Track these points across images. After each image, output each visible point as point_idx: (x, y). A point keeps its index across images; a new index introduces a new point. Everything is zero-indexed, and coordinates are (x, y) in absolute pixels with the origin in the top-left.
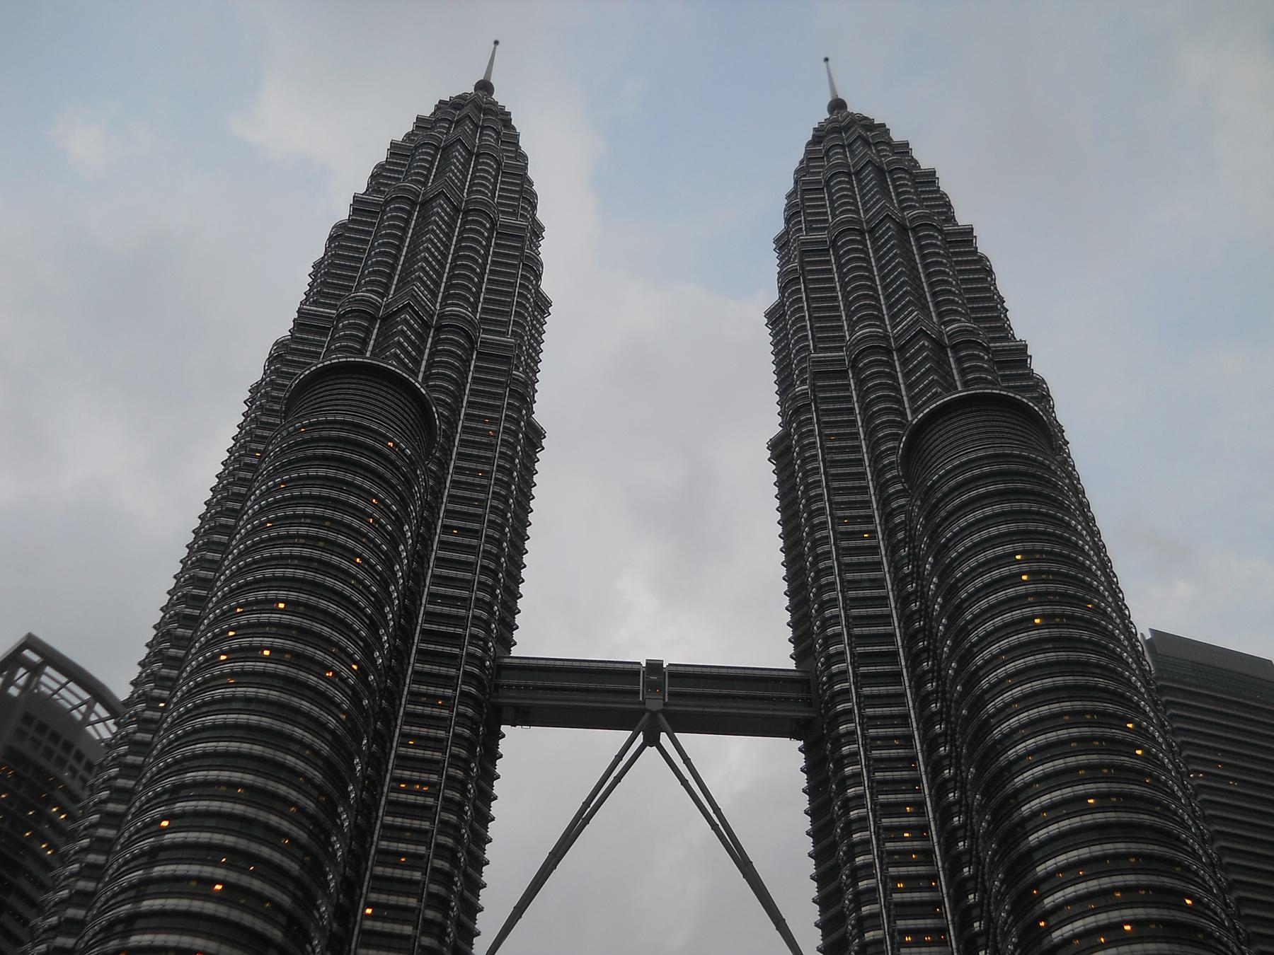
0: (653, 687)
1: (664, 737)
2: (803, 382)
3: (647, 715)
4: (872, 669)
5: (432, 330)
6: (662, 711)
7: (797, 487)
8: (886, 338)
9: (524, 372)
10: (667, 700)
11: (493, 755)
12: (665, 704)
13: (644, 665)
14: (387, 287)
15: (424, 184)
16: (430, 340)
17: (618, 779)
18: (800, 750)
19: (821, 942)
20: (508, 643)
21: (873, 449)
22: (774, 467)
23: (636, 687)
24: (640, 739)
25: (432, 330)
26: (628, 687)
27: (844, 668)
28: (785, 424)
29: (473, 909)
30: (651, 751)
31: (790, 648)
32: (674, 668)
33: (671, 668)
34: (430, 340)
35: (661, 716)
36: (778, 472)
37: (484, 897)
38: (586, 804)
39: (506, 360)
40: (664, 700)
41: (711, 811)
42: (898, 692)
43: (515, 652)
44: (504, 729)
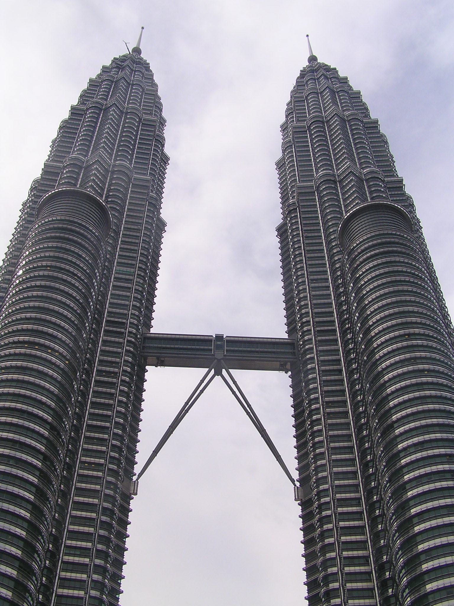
0: (218, 347)
1: (224, 372)
2: (293, 198)
3: (216, 361)
4: (324, 338)
5: (110, 173)
6: (223, 359)
7: (291, 263)
8: (334, 176)
9: (156, 193)
10: (225, 354)
13: (214, 337)
14: (87, 152)
15: (106, 100)
17: (202, 391)
18: (289, 377)
19: (299, 477)
20: (149, 326)
22: (279, 240)
24: (212, 372)
25: (110, 173)
28: (285, 218)
30: (218, 378)
31: (286, 328)
32: (229, 338)
33: (228, 338)
36: (281, 242)
39: (147, 187)
41: (246, 406)
42: (336, 348)
43: (152, 331)
44: (147, 367)
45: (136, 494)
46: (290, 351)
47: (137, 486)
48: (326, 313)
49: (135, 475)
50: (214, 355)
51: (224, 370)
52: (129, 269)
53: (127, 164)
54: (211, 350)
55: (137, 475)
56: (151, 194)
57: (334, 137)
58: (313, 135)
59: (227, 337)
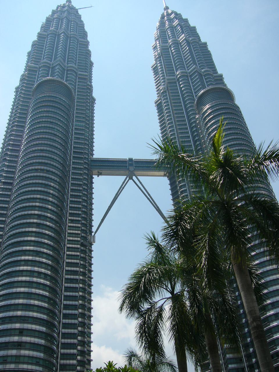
0: (131, 165)
1: (134, 178)
5: (66, 71)
13: (128, 159)
14: (51, 59)
23: (126, 165)
25: (66, 71)
29: (91, 220)
30: (131, 181)
37: (94, 217)
38: (117, 194)
45: (95, 242)
47: (95, 238)
49: (93, 232)
52: (82, 124)
55: (94, 232)
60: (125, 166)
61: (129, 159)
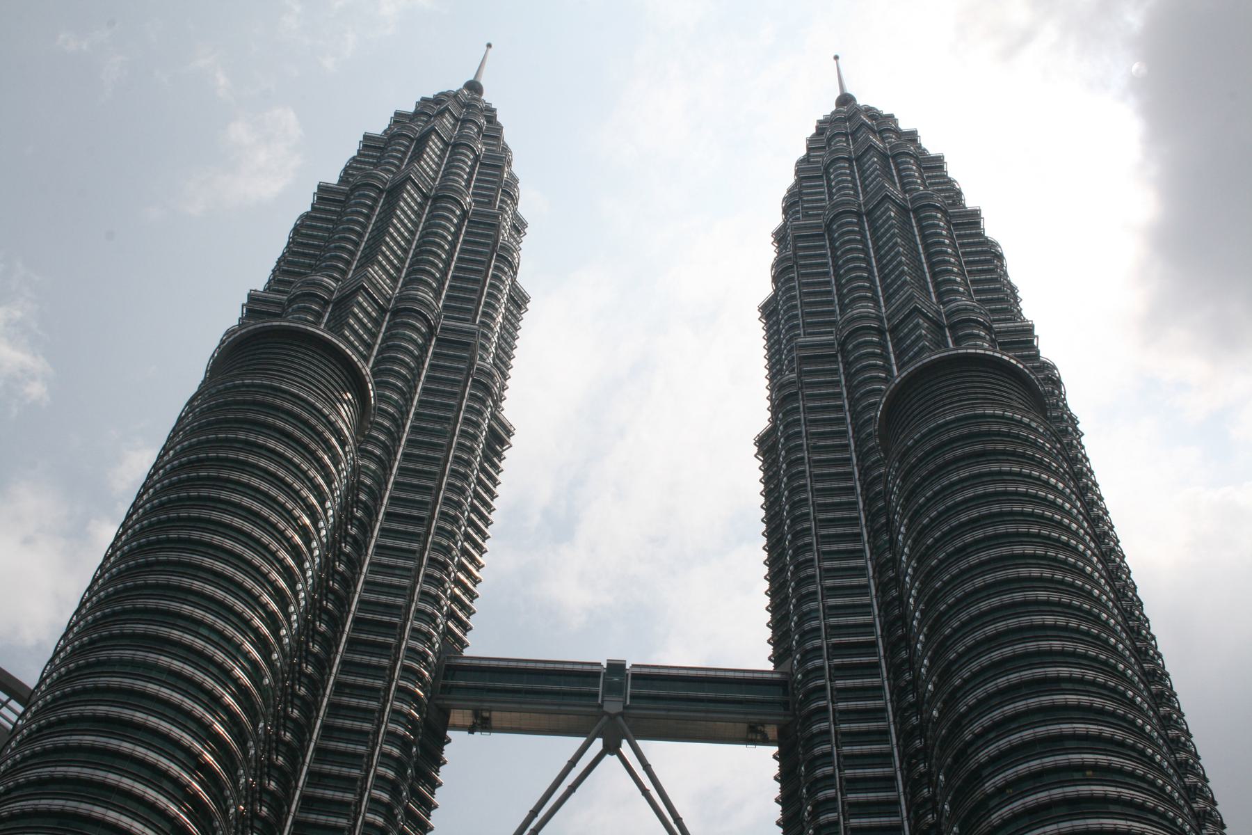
1: (625, 748)
3: (605, 718)
6: (621, 714)
10: (628, 703)
11: (437, 761)
12: (625, 707)
13: (605, 666)
16: (385, 324)
17: (572, 789)
21: (867, 490)
26: (585, 689)
27: (829, 750)
33: (637, 670)
34: (385, 324)
35: (620, 719)
40: (626, 702)
46: (777, 698)
48: (868, 733)
50: (601, 706)
51: (625, 743)
53: (429, 297)
54: (596, 695)
56: (478, 362)
57: (883, 252)
58: (843, 286)
59: (633, 666)
60: (581, 695)
61: (608, 664)
